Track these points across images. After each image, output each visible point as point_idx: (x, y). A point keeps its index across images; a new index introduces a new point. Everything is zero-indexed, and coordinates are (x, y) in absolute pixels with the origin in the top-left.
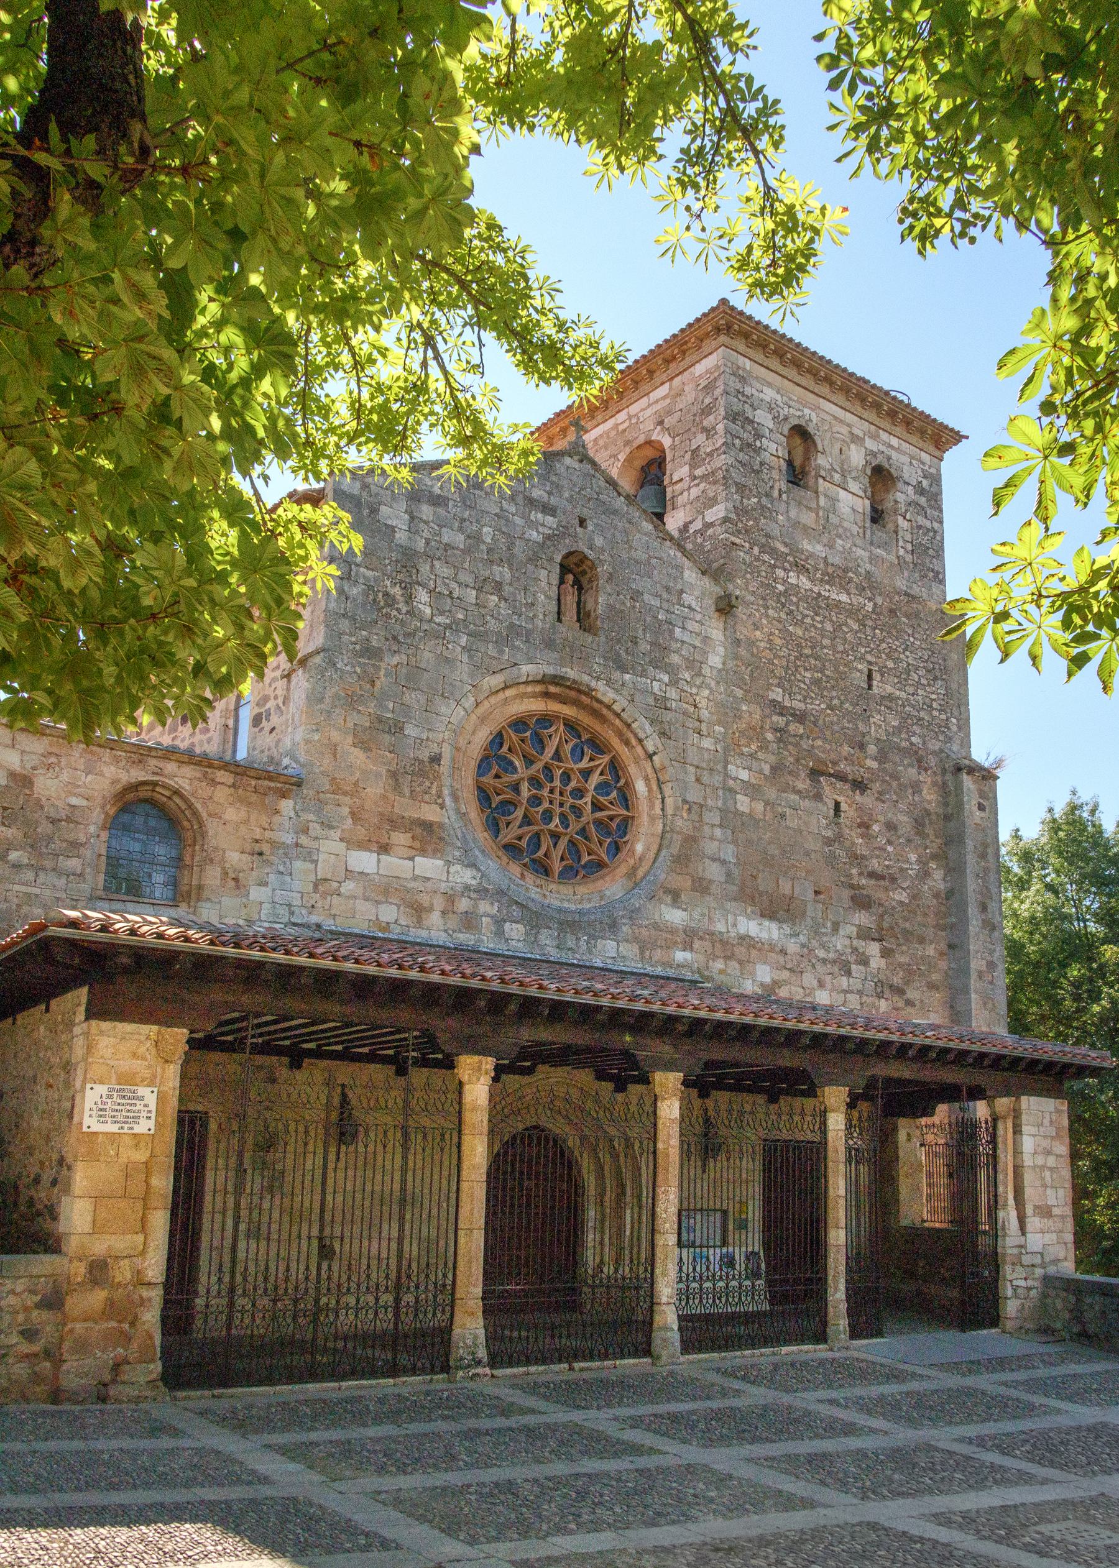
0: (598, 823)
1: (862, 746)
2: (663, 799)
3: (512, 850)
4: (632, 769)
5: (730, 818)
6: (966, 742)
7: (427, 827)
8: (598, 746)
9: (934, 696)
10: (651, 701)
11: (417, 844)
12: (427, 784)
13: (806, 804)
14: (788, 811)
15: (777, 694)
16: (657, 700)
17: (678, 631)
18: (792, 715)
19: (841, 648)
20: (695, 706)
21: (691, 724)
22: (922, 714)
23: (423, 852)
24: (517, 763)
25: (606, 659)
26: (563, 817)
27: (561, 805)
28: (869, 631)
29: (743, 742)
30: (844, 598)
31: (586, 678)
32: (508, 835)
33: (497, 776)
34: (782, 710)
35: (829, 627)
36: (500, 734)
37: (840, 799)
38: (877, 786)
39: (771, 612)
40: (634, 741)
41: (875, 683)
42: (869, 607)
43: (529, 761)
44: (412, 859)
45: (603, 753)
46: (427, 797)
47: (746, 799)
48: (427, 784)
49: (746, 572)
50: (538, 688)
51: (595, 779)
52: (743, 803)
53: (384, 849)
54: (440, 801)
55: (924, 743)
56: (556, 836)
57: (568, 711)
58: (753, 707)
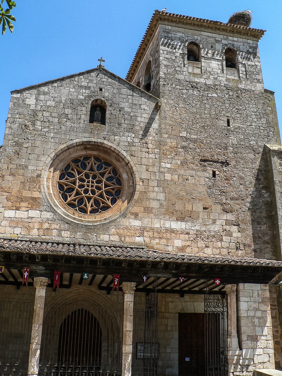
1: (226, 148)
3: (71, 205)
4: (121, 170)
9: (260, 125)
10: (127, 144)
11: (30, 206)
12: (35, 185)
13: (198, 173)
14: (190, 178)
15: (184, 134)
17: (139, 119)
20: (146, 143)
21: (145, 150)
22: (255, 132)
23: (31, 208)
25: (108, 132)
27: (92, 186)
28: (227, 105)
29: (168, 153)
30: (215, 95)
31: (99, 140)
34: (187, 139)
35: (207, 106)
37: (215, 170)
38: (233, 163)
39: (180, 106)
40: (121, 160)
41: (231, 124)
42: (227, 96)
43: (79, 173)
45: (111, 166)
46: (35, 189)
47: (170, 175)
48: (35, 185)
49: (169, 93)
50: (82, 147)
52: (168, 176)
53: (18, 209)
56: (89, 199)
57: (95, 153)
58: (172, 140)
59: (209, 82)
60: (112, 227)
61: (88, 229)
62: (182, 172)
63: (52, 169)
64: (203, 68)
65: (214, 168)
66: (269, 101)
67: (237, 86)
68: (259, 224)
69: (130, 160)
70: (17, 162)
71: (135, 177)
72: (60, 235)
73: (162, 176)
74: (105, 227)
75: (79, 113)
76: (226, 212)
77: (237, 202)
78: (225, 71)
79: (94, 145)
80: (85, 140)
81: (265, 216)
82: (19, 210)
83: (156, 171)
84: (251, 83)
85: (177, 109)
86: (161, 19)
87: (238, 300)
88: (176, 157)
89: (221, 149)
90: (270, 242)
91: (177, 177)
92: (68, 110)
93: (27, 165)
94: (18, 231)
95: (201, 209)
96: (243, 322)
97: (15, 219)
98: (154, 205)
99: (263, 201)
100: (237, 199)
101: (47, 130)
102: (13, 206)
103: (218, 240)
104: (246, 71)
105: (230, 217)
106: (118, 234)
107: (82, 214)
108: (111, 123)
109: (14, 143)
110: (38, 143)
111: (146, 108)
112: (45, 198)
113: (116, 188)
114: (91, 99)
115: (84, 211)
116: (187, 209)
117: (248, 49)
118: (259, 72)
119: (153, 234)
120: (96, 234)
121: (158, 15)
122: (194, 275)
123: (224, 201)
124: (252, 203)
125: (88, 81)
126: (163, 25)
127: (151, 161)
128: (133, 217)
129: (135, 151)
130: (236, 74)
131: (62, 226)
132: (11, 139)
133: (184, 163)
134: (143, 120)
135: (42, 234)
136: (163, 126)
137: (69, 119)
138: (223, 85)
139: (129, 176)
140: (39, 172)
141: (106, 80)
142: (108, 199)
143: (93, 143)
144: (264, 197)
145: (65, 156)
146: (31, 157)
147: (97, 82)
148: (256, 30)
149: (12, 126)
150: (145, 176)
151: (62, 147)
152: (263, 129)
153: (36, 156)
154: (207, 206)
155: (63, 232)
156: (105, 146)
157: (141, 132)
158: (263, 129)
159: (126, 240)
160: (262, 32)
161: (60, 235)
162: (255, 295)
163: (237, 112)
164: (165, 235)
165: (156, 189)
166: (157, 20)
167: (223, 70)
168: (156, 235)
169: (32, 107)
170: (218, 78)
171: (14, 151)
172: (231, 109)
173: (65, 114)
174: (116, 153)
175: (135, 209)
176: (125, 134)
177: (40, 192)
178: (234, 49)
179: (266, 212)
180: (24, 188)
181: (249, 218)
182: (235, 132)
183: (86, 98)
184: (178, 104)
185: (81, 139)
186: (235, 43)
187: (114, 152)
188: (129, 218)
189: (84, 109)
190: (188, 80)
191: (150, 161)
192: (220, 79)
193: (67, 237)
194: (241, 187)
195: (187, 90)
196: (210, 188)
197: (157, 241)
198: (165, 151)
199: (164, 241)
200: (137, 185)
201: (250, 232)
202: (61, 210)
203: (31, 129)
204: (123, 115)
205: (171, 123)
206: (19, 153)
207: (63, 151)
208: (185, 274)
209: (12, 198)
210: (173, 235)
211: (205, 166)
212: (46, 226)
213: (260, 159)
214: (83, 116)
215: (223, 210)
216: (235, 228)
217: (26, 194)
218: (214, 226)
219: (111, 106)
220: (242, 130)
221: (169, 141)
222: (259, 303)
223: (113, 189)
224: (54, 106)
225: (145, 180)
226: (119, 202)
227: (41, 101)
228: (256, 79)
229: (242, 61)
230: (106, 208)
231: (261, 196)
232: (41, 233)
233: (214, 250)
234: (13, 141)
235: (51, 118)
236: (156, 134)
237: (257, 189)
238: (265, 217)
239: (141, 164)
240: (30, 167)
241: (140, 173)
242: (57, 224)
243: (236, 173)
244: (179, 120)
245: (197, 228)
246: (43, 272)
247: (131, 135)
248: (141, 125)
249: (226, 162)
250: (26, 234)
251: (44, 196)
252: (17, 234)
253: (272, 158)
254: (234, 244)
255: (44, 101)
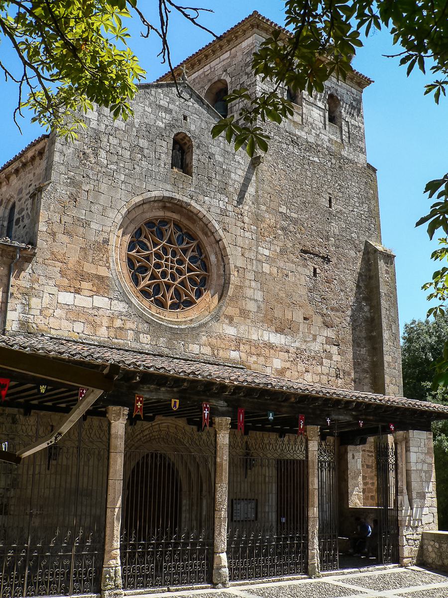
0: (190, 278)
2: (224, 265)
3: (145, 293)
4: (208, 249)
5: (259, 276)
6: (379, 239)
7: (101, 278)
8: (192, 237)
9: (362, 212)
10: (219, 212)
11: (95, 289)
12: (101, 255)
13: (299, 268)
14: (290, 274)
15: (283, 209)
16: (221, 211)
17: (233, 175)
18: (291, 220)
19: (315, 186)
20: (241, 215)
21: (240, 224)
22: (357, 221)
23: (97, 293)
24: (149, 244)
25: (195, 188)
26: (172, 275)
28: (329, 177)
29: (266, 234)
30: (316, 159)
31: (185, 199)
32: (143, 284)
33: (138, 252)
34: (286, 217)
36: (140, 229)
37: (316, 266)
38: (334, 260)
44: (92, 296)
46: (101, 263)
47: (268, 266)
48: (101, 255)
50: (160, 204)
51: (190, 254)
52: (266, 268)
53: (78, 291)
54: (107, 265)
55: (358, 237)
56: (168, 286)
57: (176, 216)
59: (311, 139)
60: (203, 334)
61: (175, 334)
62: (282, 264)
63: (121, 231)
64: (304, 117)
65: (315, 264)
66: (372, 181)
67: (340, 152)
68: (358, 347)
69: (223, 237)
70: (74, 212)
71: (229, 264)
72: (137, 340)
73: (260, 267)
74: (193, 332)
75: (158, 148)
76: (327, 326)
77: (338, 314)
78: (327, 127)
79: (176, 204)
80: (167, 194)
81: (364, 336)
82: (79, 294)
83: (252, 258)
84: (354, 150)
85: (276, 170)
86: (258, 26)
87: (408, 450)
88: (275, 242)
89: (322, 239)
90: (369, 371)
91: (275, 270)
92: (143, 140)
93: (88, 221)
94: (79, 327)
95: (301, 320)
96: (414, 477)
97: (74, 308)
98: (251, 306)
99: (362, 316)
100: (337, 311)
101: (115, 168)
102: (70, 286)
103: (318, 364)
104: (349, 133)
105: (330, 333)
106: (210, 344)
107: (161, 310)
108: (199, 175)
109: (69, 181)
110: (103, 187)
111: (241, 161)
112: (116, 279)
113: (202, 274)
114: (174, 130)
115: (161, 304)
116: (286, 317)
117: (352, 101)
118: (362, 139)
119: (250, 348)
120: (183, 343)
121: (257, 20)
122: (371, 418)
123: (325, 311)
124: (352, 318)
125: (168, 100)
126: (260, 35)
127: (247, 242)
128: (227, 321)
129: (228, 224)
130: (338, 135)
131: (140, 326)
132: (64, 172)
133: (283, 251)
134: (237, 178)
135: (113, 336)
136: (260, 193)
137: (144, 156)
138: (325, 147)
139: (219, 260)
140: (105, 235)
141: (191, 104)
142: (192, 290)
143: (176, 202)
144: (364, 312)
145: (137, 215)
146: (94, 208)
147: (180, 104)
148: (363, 76)
149: (64, 150)
150: (240, 263)
151: (138, 199)
152: (365, 218)
153: (101, 208)
154: (308, 316)
155: (141, 335)
156: (192, 209)
157: (236, 198)
158: (365, 218)
159: (220, 354)
160: (369, 82)
161: (137, 340)
162: (422, 445)
163: (339, 189)
164: (263, 352)
165: (253, 284)
166: (252, 26)
167: (325, 124)
168: (253, 350)
169: (94, 124)
170: (320, 135)
171: (68, 193)
172: (333, 183)
173: (139, 146)
174: (203, 222)
175: (230, 310)
176: (216, 195)
177: (109, 268)
178: (337, 98)
179: (365, 330)
180: (85, 258)
181: (350, 338)
182: (337, 218)
183: (167, 128)
184: (277, 164)
185: (162, 192)
186: (339, 89)
187: (201, 219)
188: (223, 322)
189: (164, 144)
190: (287, 130)
191: (247, 242)
192: (323, 138)
193: (147, 344)
194: (342, 294)
195: (287, 144)
196: (310, 290)
197: (254, 358)
198: (263, 230)
199: (261, 360)
200: (231, 276)
201: (350, 356)
202: (134, 301)
203: (93, 162)
204: (214, 165)
205: (270, 190)
206: (76, 199)
207: (138, 206)
208: (364, 417)
209: (68, 272)
210: (272, 351)
211: (306, 259)
212: (118, 323)
213: (361, 259)
214: (163, 156)
215: (324, 323)
216: (334, 350)
217: (89, 268)
218: (314, 344)
219: (198, 147)
220: (344, 216)
221: (267, 215)
222: (425, 454)
223: (198, 276)
224: (124, 129)
225: (241, 269)
226: (207, 296)
227: (106, 117)
228: (359, 147)
229: (346, 117)
230: (190, 303)
231: (360, 309)
232: (112, 334)
233: (314, 375)
234: (66, 176)
235: (120, 149)
236: (253, 203)
237: (358, 301)
238: (365, 338)
239: (236, 245)
240: (93, 226)
241: (235, 259)
242: (134, 323)
243: (338, 275)
244: (278, 188)
245: (297, 344)
246: (224, 409)
247: (224, 198)
248: (235, 186)
249: (327, 258)
250: (91, 334)
251: (114, 274)
252: (78, 333)
253: (379, 262)
254: (334, 370)
255: (109, 118)
